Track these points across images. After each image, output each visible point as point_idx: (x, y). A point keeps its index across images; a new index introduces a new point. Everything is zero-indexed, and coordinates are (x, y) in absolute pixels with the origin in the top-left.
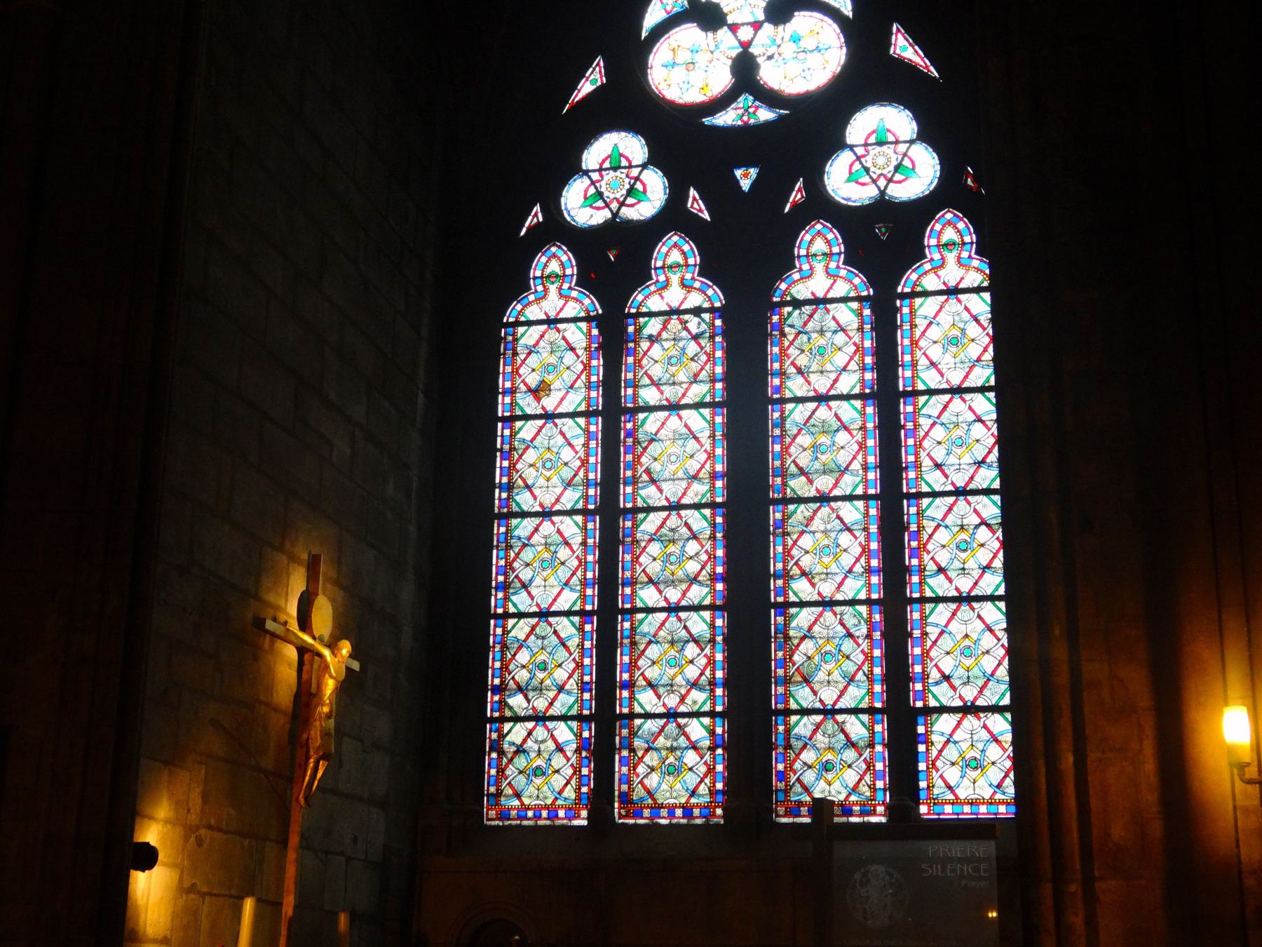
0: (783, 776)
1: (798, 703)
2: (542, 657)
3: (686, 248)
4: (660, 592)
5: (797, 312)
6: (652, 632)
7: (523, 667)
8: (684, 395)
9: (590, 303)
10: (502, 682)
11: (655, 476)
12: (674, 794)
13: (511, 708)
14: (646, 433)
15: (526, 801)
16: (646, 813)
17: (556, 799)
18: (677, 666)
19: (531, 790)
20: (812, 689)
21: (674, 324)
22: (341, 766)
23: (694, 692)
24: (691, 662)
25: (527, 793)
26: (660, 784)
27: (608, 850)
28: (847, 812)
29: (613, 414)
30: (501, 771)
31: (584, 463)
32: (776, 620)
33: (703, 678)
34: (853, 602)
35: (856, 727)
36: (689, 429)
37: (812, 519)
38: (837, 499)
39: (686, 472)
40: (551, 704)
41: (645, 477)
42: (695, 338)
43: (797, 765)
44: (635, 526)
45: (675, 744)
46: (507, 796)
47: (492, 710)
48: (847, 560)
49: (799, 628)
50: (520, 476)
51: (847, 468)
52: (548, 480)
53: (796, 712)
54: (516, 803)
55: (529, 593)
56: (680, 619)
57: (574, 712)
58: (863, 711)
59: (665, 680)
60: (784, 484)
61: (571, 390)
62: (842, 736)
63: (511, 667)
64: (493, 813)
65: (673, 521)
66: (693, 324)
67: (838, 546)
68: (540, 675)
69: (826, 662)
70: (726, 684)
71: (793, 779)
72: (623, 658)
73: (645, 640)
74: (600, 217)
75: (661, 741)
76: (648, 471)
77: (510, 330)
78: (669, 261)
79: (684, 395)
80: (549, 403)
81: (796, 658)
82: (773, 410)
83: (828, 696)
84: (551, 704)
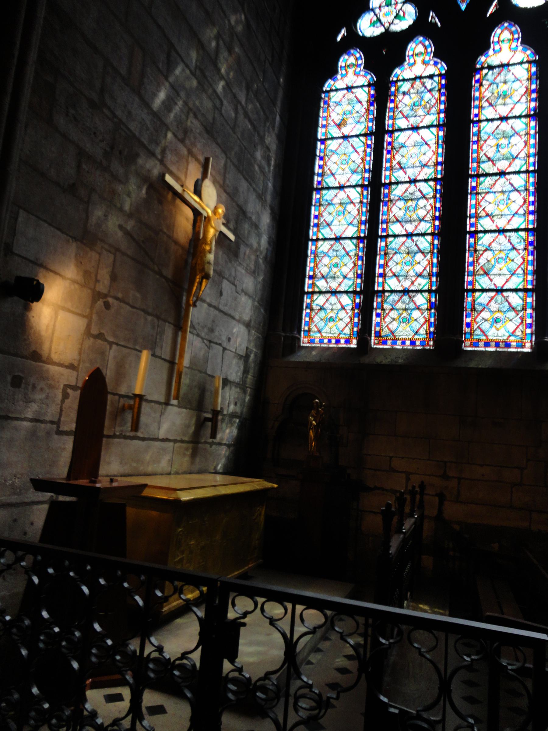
0: (469, 325)
1: (480, 286)
2: (335, 260)
3: (427, 43)
4: (403, 226)
5: (491, 72)
6: (397, 247)
7: (325, 265)
8: (422, 121)
9: (370, 77)
10: (314, 274)
11: (403, 166)
12: (406, 333)
13: (318, 287)
14: (399, 143)
15: (324, 335)
16: (389, 342)
17: (340, 334)
18: (410, 265)
19: (327, 329)
20: (489, 278)
21: (418, 82)
22: (221, 294)
23: (419, 279)
24: (419, 263)
25: (324, 331)
26: (398, 327)
27: (361, 367)
28: (508, 345)
29: (380, 135)
30: (311, 319)
31: (363, 160)
32: (470, 241)
33: (425, 272)
34: (517, 230)
35: (516, 299)
36: (424, 140)
37: (494, 184)
38: (509, 173)
39: (420, 162)
40: (340, 285)
41: (397, 166)
42: (430, 91)
43: (479, 319)
44: (390, 192)
45: (407, 307)
46: (314, 332)
47: (308, 288)
48: (514, 207)
49: (483, 245)
50: (329, 169)
51: (517, 157)
52: (343, 170)
53: (479, 290)
54: (318, 335)
55: (330, 229)
56: (413, 241)
57: (351, 289)
58: (520, 290)
59: (403, 273)
60: (478, 167)
61: (359, 124)
62: (507, 304)
63: (319, 266)
64: (306, 340)
65: (412, 188)
66: (429, 84)
67: (509, 199)
68: (335, 270)
69: (498, 263)
70: (438, 275)
71: (476, 327)
72: (380, 261)
73: (393, 252)
74: (378, 31)
75: (399, 305)
76: (399, 163)
77: (327, 94)
78: (417, 51)
79: (422, 121)
80: (346, 131)
81: (480, 261)
82: (473, 126)
83: (499, 282)
84: (340, 285)
